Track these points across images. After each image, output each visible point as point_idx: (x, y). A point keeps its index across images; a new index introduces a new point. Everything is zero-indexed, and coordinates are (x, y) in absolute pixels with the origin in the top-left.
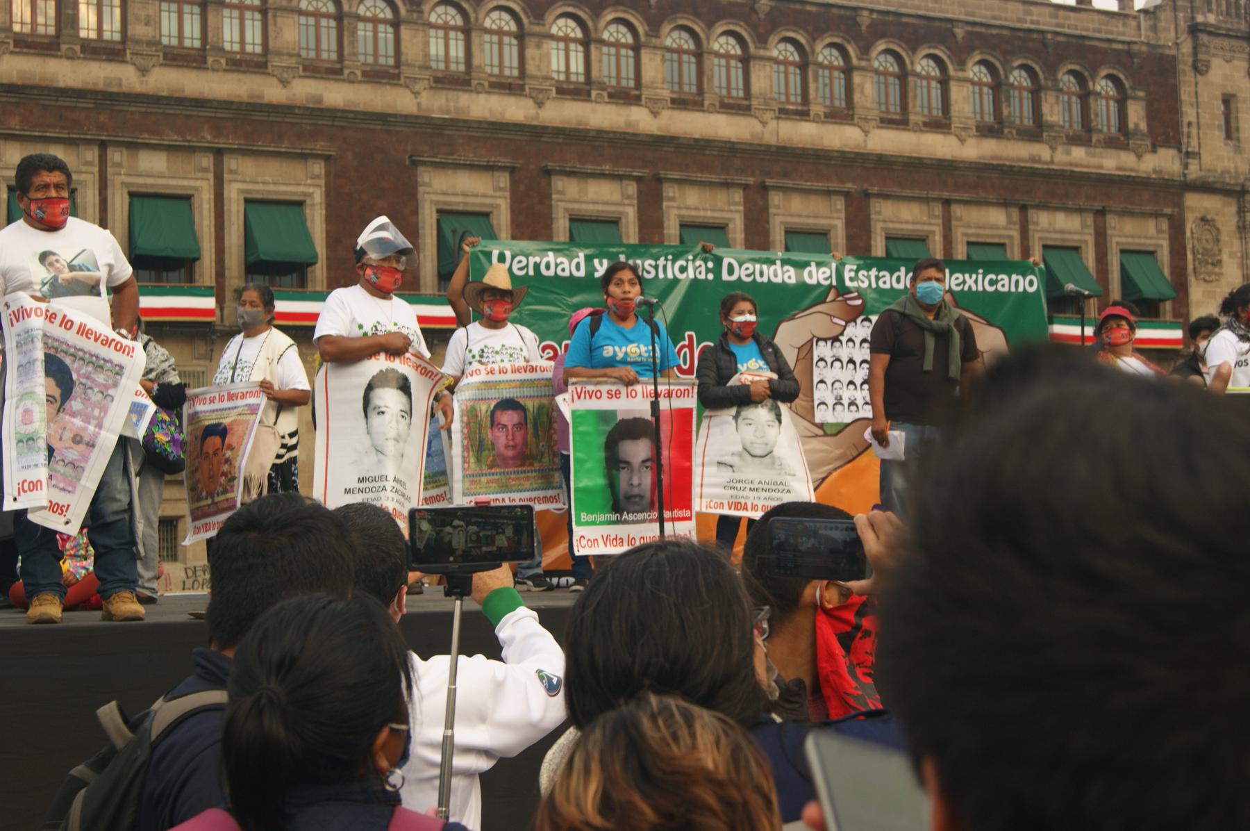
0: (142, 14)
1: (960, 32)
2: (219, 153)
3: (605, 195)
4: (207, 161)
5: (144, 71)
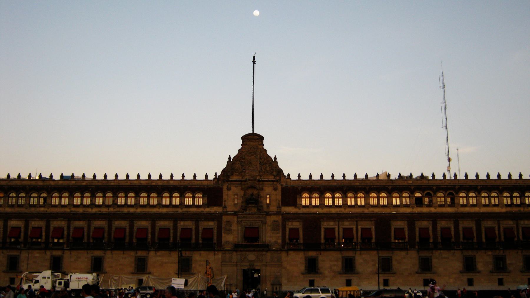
1: (501, 187)
2: (357, 221)
3: (425, 224)
4: (355, 223)
5: (345, 209)
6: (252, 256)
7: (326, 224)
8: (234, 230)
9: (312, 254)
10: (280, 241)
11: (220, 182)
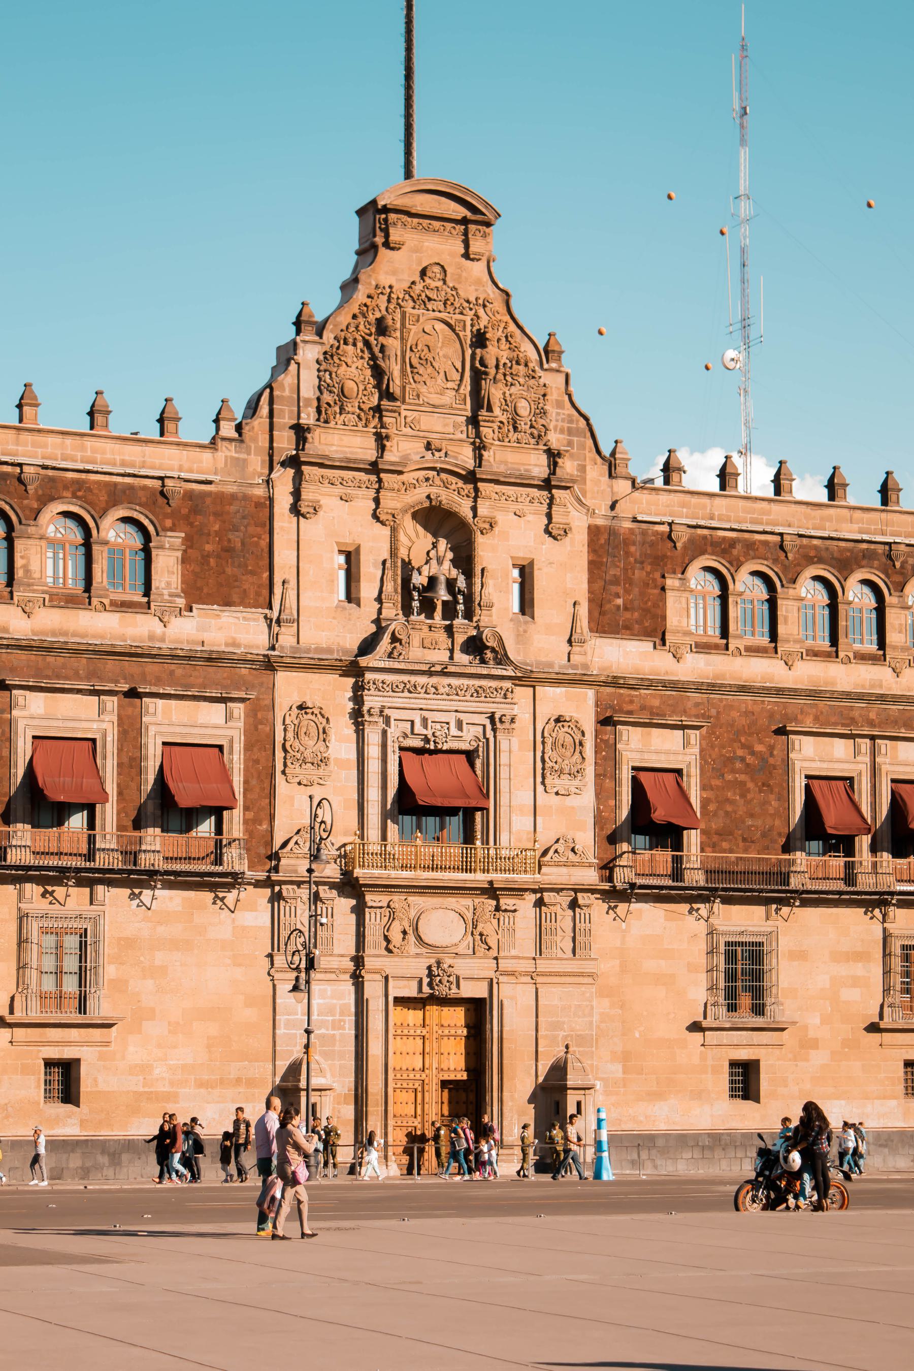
0: (897, 623)
6: (444, 923)
7: (812, 755)
8: (341, 764)
9: (743, 920)
10: (586, 839)
11: (257, 463)
